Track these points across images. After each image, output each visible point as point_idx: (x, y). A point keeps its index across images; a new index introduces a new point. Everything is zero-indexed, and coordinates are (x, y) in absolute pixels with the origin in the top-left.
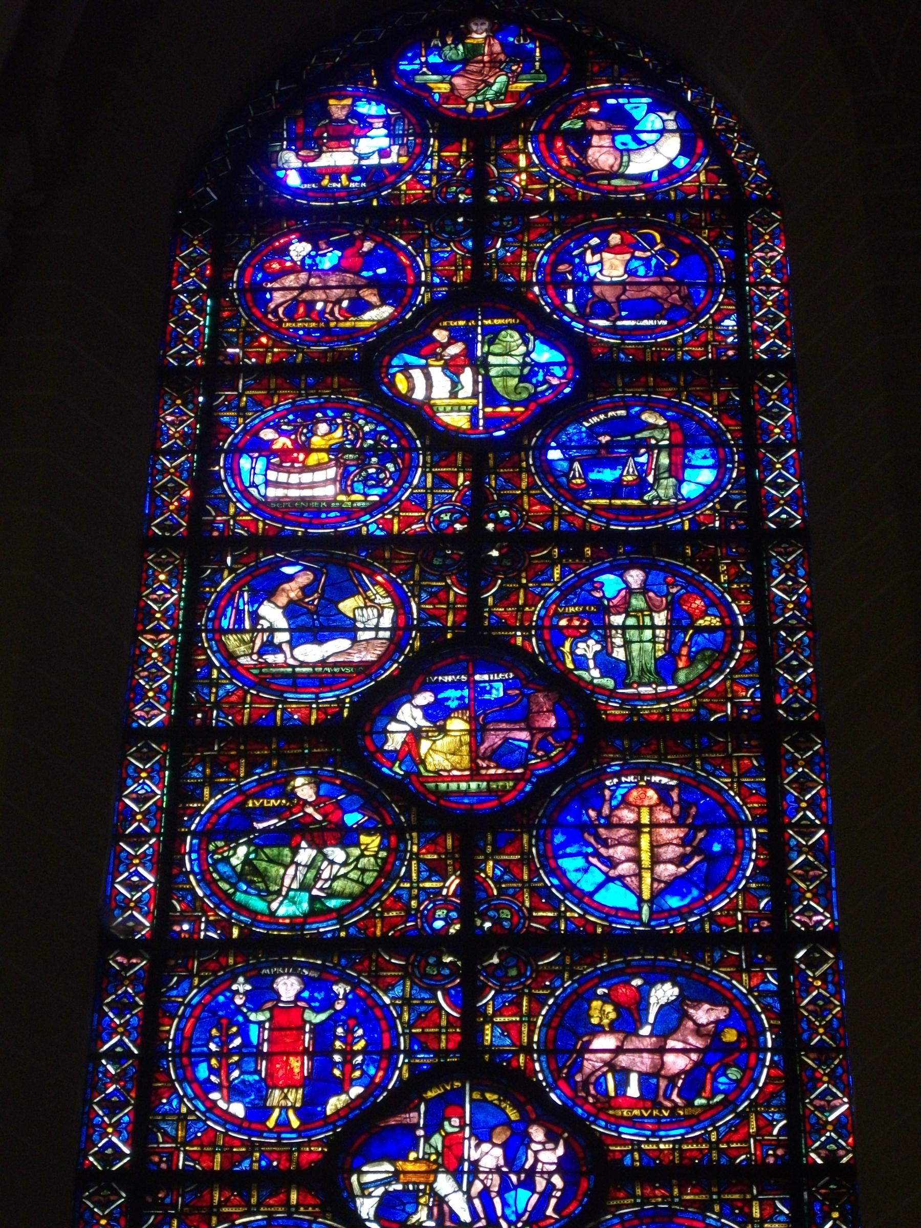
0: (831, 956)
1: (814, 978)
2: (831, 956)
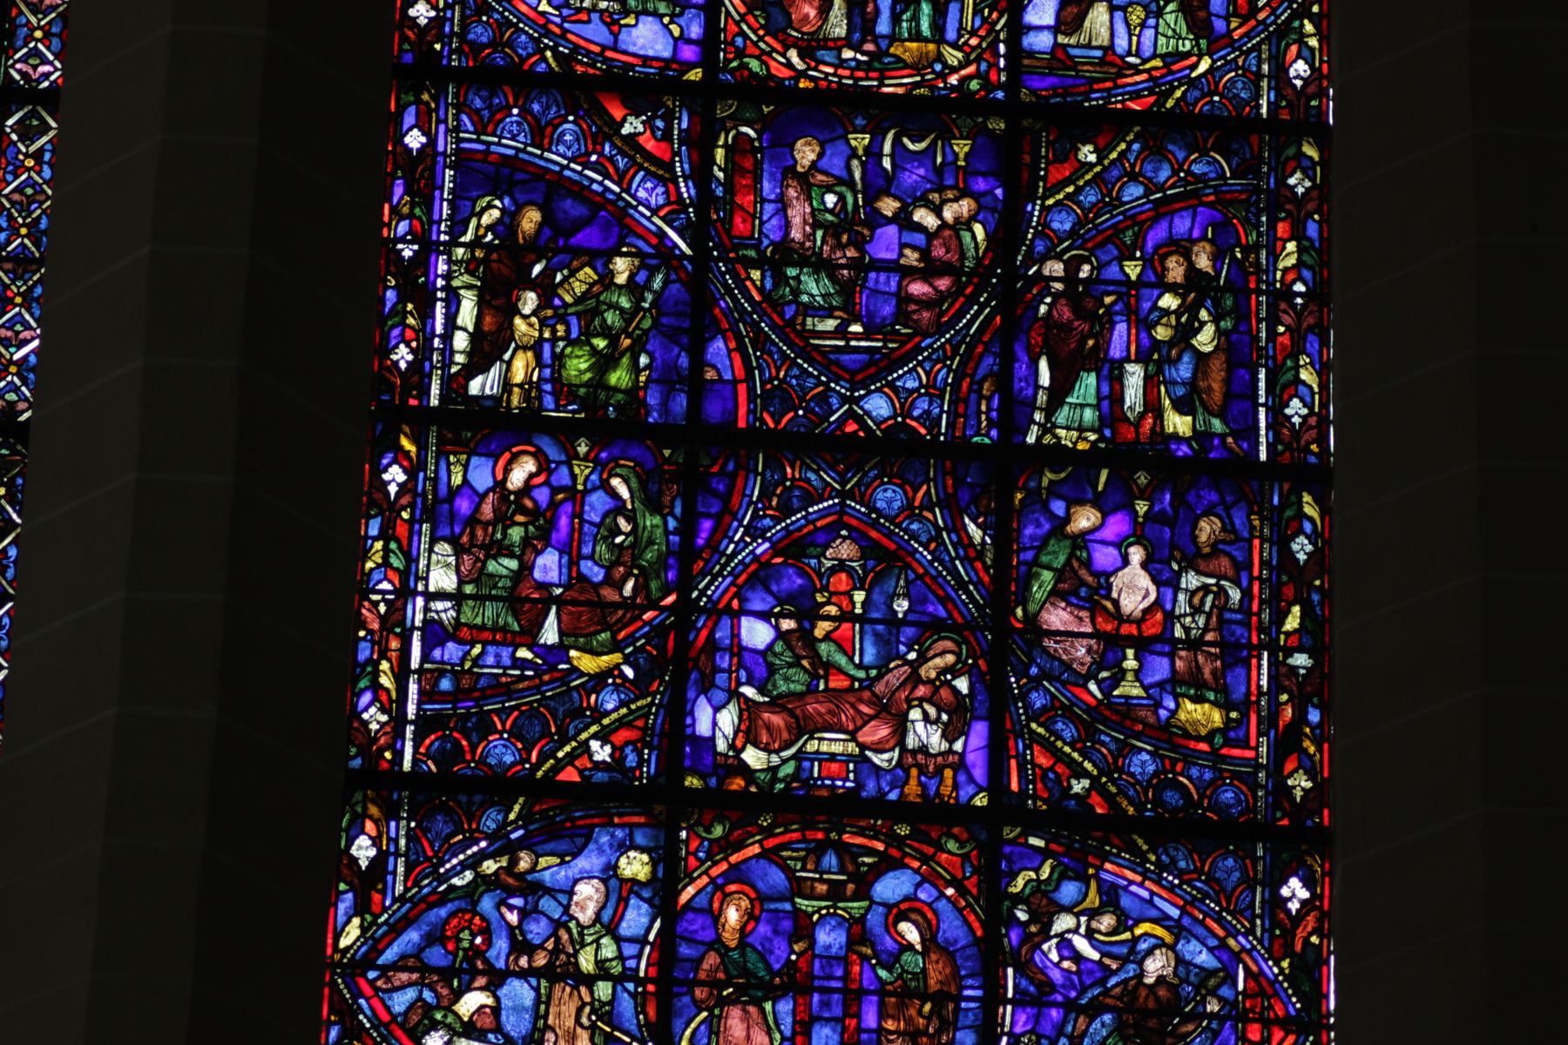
0: (54, 125)
1: (27, 155)
2: (54, 125)
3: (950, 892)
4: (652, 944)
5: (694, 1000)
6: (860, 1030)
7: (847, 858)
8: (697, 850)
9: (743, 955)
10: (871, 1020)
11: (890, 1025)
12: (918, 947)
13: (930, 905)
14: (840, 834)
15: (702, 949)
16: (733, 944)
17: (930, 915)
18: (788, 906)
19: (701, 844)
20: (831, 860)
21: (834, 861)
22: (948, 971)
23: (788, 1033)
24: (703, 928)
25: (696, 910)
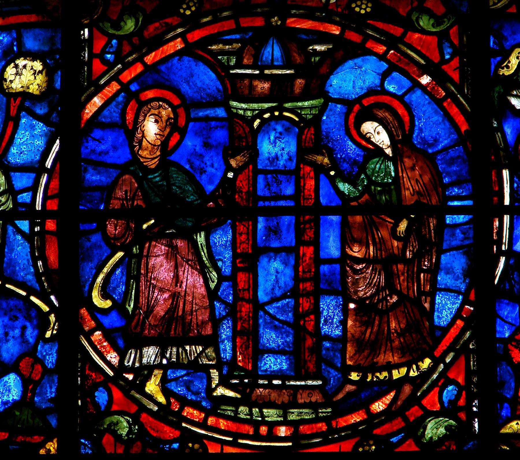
3: (425, 80)
4: (50, 172)
5: (106, 237)
6: (318, 261)
7: (294, 47)
8: (104, 52)
9: (166, 177)
10: (332, 247)
11: (356, 252)
12: (389, 151)
13: (400, 98)
14: (283, 19)
15: (114, 173)
16: (153, 164)
17: (401, 111)
18: (221, 112)
19: (109, 42)
20: (273, 51)
21: (277, 53)
22: (426, 178)
23: (227, 270)
24: (115, 148)
25: (104, 126)
